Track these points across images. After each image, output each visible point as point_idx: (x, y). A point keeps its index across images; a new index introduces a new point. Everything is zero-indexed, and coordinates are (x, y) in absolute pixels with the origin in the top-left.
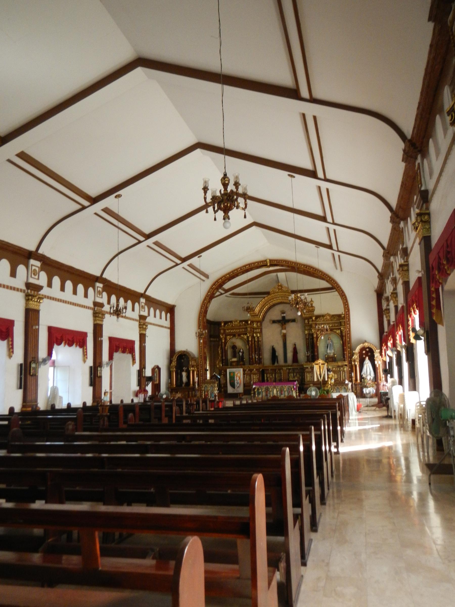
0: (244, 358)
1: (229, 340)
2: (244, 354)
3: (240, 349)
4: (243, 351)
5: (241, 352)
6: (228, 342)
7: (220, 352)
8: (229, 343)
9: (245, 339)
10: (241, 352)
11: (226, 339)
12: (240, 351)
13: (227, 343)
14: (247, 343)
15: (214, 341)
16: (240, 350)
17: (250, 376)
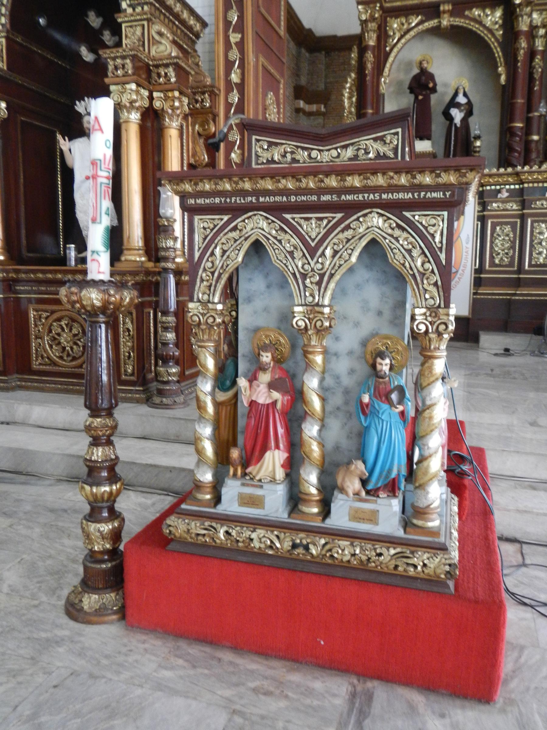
0: (478, 137)
1: (399, 40)
2: (471, 120)
3: (451, 93)
4: (469, 103)
5: (458, 105)
6: (395, 50)
7: (350, 107)
8: (393, 66)
9: (490, 31)
10: (458, 105)
11: (387, 36)
12: (453, 103)
13: (387, 55)
14: (498, 52)
15: (309, 114)
16: (456, 94)
17: (513, 226)
